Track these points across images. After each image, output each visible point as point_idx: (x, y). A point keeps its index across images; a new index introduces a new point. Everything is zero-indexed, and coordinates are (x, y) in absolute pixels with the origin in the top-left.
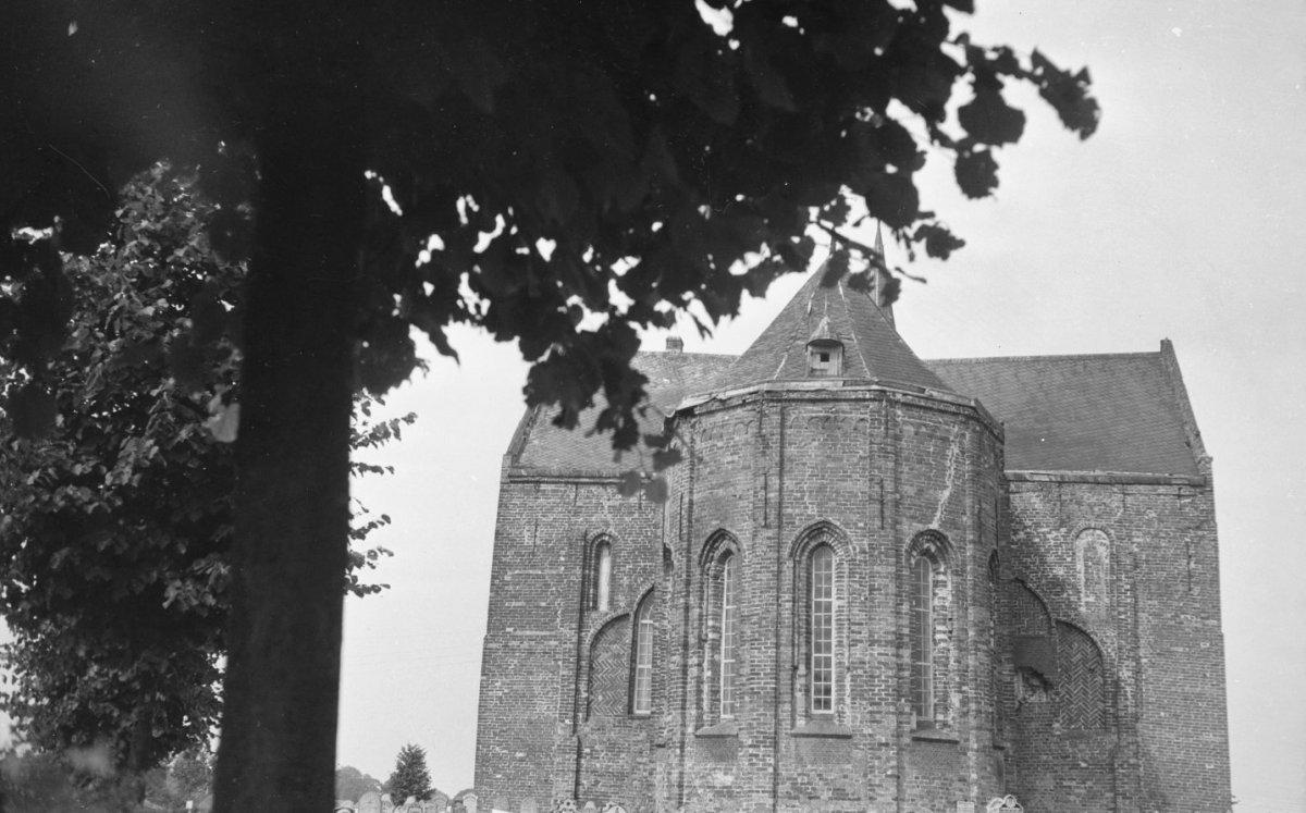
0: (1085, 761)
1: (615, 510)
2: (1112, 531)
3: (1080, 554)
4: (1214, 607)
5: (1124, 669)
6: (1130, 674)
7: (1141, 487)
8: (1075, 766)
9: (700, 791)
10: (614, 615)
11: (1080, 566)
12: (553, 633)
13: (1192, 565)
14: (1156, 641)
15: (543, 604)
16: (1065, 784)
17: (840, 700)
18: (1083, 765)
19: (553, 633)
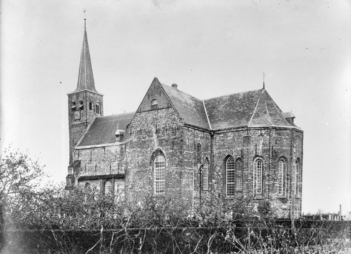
1: (202, 138)
9: (279, 209)
10: (201, 165)
12: (192, 169)
15: (191, 161)
17: (297, 192)
19: (192, 169)
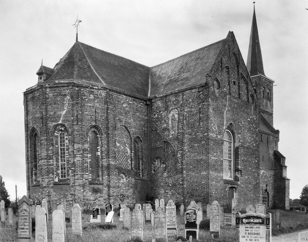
0: (171, 184)
2: (179, 109)
3: (170, 119)
4: (206, 129)
5: (179, 154)
6: (180, 155)
7: (188, 91)
8: (169, 186)
11: (170, 123)
13: (201, 115)
14: (190, 143)
16: (167, 191)
18: (171, 185)
